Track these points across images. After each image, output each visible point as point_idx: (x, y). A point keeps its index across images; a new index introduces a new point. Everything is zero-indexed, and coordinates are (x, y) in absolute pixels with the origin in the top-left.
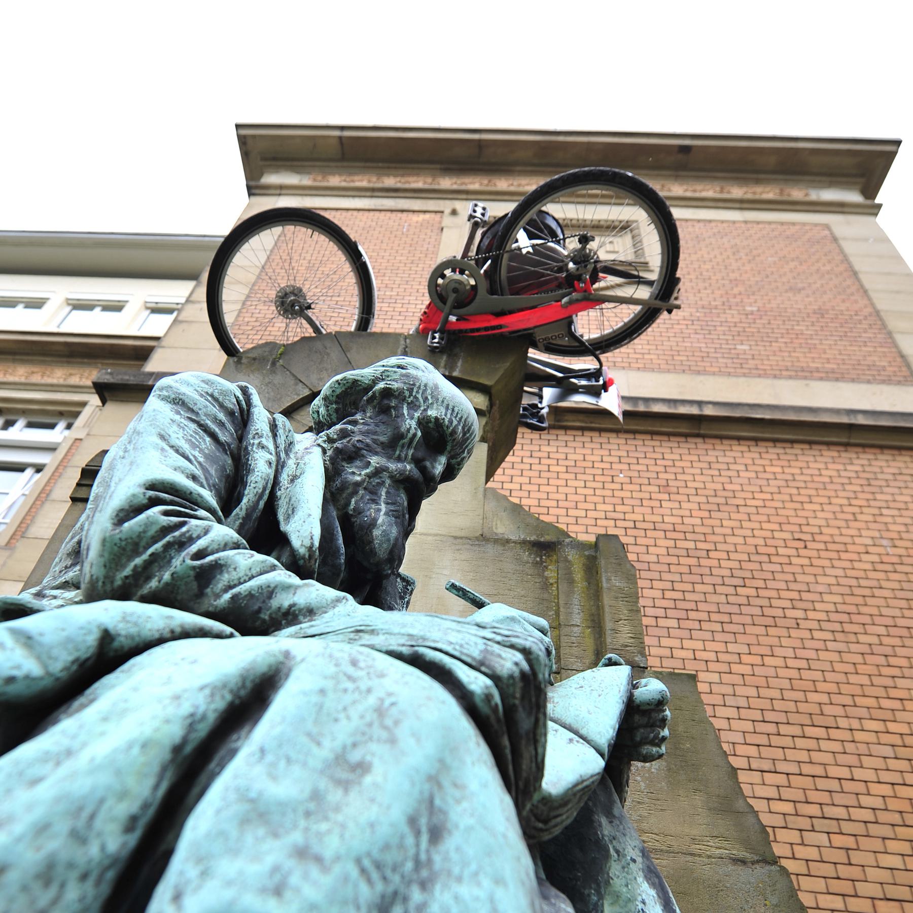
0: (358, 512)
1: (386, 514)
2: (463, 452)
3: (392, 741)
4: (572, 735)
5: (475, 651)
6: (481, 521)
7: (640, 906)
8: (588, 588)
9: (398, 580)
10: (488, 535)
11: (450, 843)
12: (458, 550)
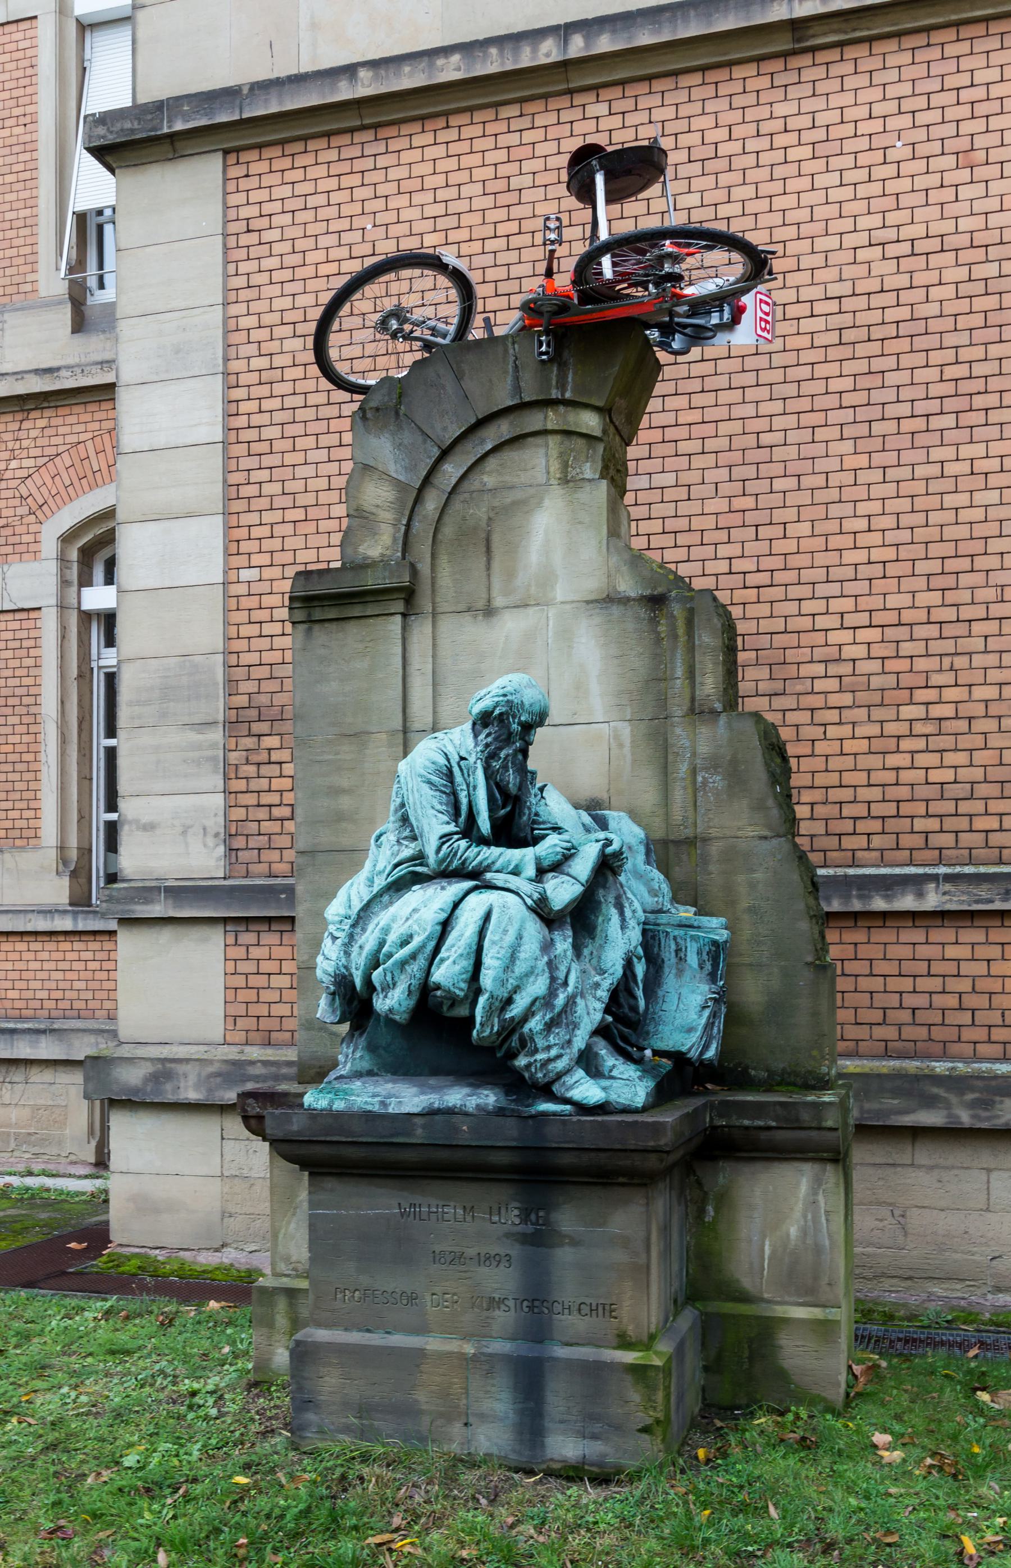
8: (688, 641)
10: (612, 595)
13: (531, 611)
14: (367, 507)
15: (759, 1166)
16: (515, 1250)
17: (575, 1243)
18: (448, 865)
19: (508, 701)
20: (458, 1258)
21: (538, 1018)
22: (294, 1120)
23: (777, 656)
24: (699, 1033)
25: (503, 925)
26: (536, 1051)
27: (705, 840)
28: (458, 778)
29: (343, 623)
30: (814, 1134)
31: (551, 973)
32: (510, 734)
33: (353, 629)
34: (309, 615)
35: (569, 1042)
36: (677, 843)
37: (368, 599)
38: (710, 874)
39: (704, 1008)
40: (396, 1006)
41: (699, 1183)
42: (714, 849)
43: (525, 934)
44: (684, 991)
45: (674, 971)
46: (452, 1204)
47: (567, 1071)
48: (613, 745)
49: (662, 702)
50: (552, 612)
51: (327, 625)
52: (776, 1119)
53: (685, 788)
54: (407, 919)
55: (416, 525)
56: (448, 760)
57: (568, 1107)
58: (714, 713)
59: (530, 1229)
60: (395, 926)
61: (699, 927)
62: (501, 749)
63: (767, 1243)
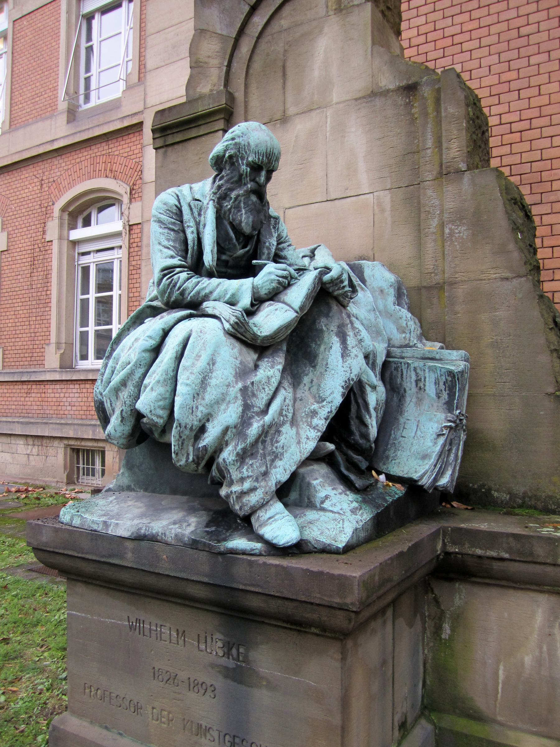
0: (234, 220)
1: (246, 213)
2: (272, 163)
3: (205, 350)
4: (288, 308)
5: (227, 318)
6: (371, 80)
7: (331, 345)
9: (272, 219)
11: (216, 365)
12: (359, 109)
13: (314, 114)
14: (203, 58)
15: (494, 592)
16: (219, 682)
17: (272, 686)
18: (169, 297)
19: (236, 144)
20: (172, 679)
21: (230, 448)
22: (44, 531)
23: (536, 177)
24: (432, 460)
25: (197, 350)
26: (231, 483)
27: (452, 284)
28: (187, 215)
29: (185, 144)
30: (549, 569)
31: (244, 400)
32: (241, 176)
33: (192, 146)
34: (165, 141)
35: (265, 474)
36: (429, 288)
37: (200, 123)
38: (456, 313)
39: (439, 435)
40: (113, 432)
41: (436, 601)
42: (460, 291)
43: (219, 360)
44: (423, 419)
45: (414, 400)
46: (168, 625)
47: (263, 505)
48: (377, 211)
49: (416, 170)
50: (329, 112)
51: (176, 147)
52: (509, 550)
53: (435, 241)
54: (130, 348)
55: (235, 65)
56: (179, 201)
57: (258, 546)
58: (459, 172)
59: (231, 663)
60: (122, 355)
61: (441, 360)
62: (231, 190)
63: (501, 667)
